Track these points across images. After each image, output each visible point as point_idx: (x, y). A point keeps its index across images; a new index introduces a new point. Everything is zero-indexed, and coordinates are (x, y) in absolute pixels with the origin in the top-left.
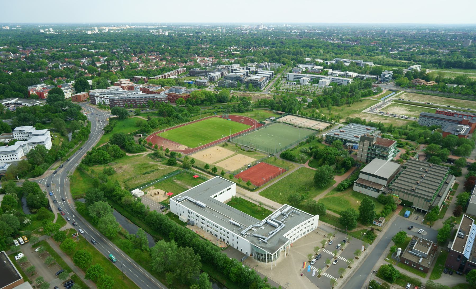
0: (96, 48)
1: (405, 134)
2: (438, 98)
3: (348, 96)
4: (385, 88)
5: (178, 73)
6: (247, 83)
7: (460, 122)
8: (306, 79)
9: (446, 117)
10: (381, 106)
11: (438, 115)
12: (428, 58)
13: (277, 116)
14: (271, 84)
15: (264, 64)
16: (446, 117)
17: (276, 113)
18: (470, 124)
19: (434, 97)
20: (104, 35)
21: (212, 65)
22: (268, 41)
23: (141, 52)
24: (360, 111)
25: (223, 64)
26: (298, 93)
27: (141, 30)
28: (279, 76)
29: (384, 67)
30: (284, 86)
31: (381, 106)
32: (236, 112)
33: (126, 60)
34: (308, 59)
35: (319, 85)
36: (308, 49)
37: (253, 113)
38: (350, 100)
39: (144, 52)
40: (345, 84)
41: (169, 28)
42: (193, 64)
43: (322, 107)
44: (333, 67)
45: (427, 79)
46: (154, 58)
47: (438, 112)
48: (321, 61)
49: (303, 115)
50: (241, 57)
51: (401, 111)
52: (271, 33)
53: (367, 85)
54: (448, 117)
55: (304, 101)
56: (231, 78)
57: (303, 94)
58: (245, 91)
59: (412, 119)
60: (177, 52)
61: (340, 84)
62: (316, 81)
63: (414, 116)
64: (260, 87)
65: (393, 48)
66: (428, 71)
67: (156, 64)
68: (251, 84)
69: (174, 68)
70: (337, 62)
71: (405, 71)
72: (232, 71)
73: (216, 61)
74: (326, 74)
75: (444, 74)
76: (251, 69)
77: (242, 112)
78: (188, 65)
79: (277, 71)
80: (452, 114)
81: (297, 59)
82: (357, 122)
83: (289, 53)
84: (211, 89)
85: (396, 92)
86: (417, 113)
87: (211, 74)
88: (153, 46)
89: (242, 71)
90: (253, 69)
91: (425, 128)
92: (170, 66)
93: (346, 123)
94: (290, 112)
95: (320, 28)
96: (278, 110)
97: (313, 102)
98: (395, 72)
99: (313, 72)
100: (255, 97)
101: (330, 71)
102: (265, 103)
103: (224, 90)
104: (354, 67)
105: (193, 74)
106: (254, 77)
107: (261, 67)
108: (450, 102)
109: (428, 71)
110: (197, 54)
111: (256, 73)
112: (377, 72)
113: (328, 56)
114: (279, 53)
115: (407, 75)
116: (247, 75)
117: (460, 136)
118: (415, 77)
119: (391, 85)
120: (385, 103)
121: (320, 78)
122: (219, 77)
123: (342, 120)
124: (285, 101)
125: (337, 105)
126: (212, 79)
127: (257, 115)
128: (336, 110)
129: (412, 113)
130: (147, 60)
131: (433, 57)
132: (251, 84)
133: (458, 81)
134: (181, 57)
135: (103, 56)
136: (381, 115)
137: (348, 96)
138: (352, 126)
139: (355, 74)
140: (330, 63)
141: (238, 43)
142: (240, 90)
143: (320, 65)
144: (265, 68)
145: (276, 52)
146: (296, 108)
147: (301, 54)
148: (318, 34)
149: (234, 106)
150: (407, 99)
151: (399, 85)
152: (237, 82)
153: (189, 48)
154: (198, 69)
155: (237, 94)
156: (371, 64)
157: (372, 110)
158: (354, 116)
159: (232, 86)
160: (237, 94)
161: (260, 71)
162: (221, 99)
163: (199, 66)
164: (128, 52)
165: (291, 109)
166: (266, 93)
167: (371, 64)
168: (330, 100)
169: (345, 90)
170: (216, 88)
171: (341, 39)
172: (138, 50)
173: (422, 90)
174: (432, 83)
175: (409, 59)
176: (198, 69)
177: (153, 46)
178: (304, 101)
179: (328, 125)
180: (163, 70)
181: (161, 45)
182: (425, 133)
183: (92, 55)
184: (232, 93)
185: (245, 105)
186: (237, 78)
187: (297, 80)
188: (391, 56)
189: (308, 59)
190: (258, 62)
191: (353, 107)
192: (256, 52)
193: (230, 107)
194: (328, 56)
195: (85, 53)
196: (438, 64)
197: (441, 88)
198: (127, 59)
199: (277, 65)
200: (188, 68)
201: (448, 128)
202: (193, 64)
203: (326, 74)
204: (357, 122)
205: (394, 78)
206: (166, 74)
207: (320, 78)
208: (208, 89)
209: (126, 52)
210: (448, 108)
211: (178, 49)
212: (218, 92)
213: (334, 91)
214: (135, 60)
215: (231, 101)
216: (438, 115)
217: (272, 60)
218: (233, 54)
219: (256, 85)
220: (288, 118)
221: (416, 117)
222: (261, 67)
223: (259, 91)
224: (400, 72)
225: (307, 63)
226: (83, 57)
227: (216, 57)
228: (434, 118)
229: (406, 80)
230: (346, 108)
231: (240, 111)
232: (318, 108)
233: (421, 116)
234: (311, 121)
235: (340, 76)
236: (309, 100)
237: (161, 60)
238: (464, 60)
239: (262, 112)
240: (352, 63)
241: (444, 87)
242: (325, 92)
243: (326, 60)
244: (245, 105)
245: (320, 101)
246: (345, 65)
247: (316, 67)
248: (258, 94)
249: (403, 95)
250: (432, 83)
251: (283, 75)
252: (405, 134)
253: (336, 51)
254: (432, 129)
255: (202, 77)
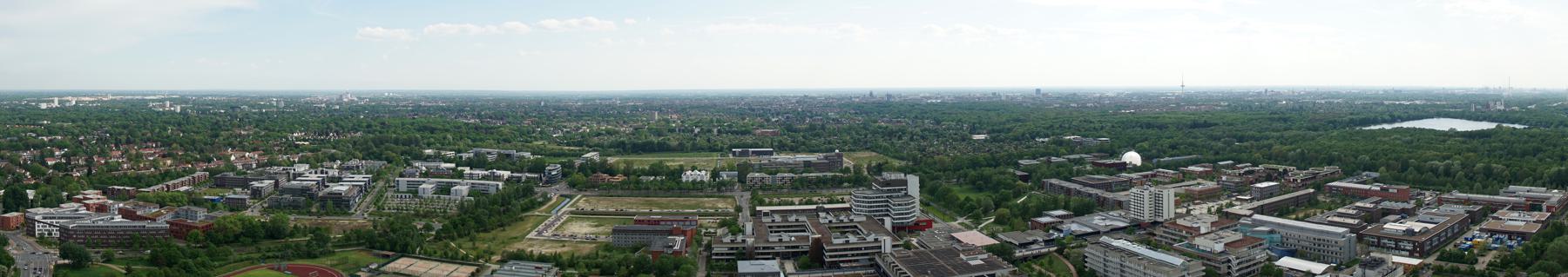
0: (50, 133)
1: (597, 266)
2: (633, 200)
3: (499, 213)
4: (554, 193)
5: (193, 182)
6: (324, 199)
7: (671, 233)
8: (428, 186)
9: (651, 228)
10: (553, 224)
11: (638, 227)
12: (607, 140)
13: (382, 261)
14: (368, 199)
15: (354, 163)
16: (651, 228)
17: (378, 255)
18: (684, 233)
19: (627, 199)
20: (68, 110)
21: (258, 166)
22: (360, 121)
23: (128, 142)
24: (523, 237)
25: (279, 165)
26: (417, 215)
27: (133, 103)
28: (381, 184)
29: (547, 160)
30: (392, 202)
31: (553, 224)
32: (301, 257)
33: (100, 155)
34: (428, 151)
35: (452, 197)
36: (427, 134)
37: (336, 257)
38: (504, 219)
39: (134, 143)
40: (493, 191)
41: (183, 100)
42: (222, 164)
43: (460, 236)
44: (471, 164)
45: (612, 172)
46: (151, 153)
47: (637, 222)
48: (451, 154)
49: (428, 256)
50: (312, 151)
51: (582, 229)
52: (364, 108)
53: (528, 191)
54: (654, 227)
55: (428, 228)
56: (293, 191)
57: (425, 216)
58: (318, 214)
59: (602, 238)
60: (194, 142)
61: (485, 193)
62: (445, 190)
63: (603, 232)
64: (348, 207)
65: (556, 128)
66: (611, 160)
67: (154, 164)
68: (330, 202)
69: (186, 172)
70: (476, 154)
71: (578, 162)
72: (296, 176)
73: (265, 159)
74: (461, 175)
75: (632, 163)
76: (331, 173)
77: (315, 257)
78: (212, 166)
79: (377, 176)
80: (657, 222)
81: (411, 152)
82: (519, 257)
83: (396, 142)
84: (253, 213)
85: (571, 197)
86: (609, 229)
87: (256, 184)
88: (152, 132)
89: (314, 177)
90: (334, 173)
91: (624, 251)
92: (180, 169)
93: (502, 262)
94: (405, 251)
95: (444, 99)
96: (383, 249)
97: (445, 229)
98: (563, 164)
99: (439, 174)
100: (339, 224)
101: (467, 170)
102: (358, 238)
103: (280, 215)
104: (504, 161)
105: (222, 183)
106: (336, 188)
107: (348, 168)
108: (651, 204)
109: (611, 160)
110: (230, 145)
111: (338, 180)
112: (538, 168)
113: (462, 145)
114: (379, 142)
115: (582, 168)
116: (322, 184)
117: (676, 253)
118: (594, 171)
119: (562, 187)
120: (558, 219)
121: (452, 185)
122: (271, 189)
123: (496, 258)
124: (394, 231)
125: (486, 231)
126: (256, 194)
127: (344, 262)
128: (483, 240)
129: (601, 229)
130: (139, 157)
131: (613, 138)
132: (330, 202)
133: (654, 171)
134: (201, 151)
135: (61, 148)
136: (557, 239)
137: (499, 213)
138: (512, 266)
139: (506, 174)
140: (465, 156)
141: (305, 126)
142: (310, 214)
143: (449, 161)
144: (356, 170)
145: (373, 141)
146: (414, 243)
147: (417, 142)
148: (443, 109)
149: (297, 245)
150: (588, 208)
151: (572, 185)
152: (306, 199)
153: (217, 136)
154: (231, 175)
155: (305, 221)
156: (527, 155)
157: (540, 233)
158: (515, 247)
159: (295, 207)
160: (305, 221)
161: (347, 175)
162: (274, 232)
163: (234, 169)
164: (105, 141)
165: (406, 245)
166: (360, 218)
167: (527, 155)
168: (472, 223)
169: (494, 202)
170: (265, 211)
171: (479, 116)
172: (123, 138)
173: (608, 190)
174: (620, 178)
175: (580, 144)
176: (231, 175)
177: (152, 132)
178: (428, 228)
179: (473, 269)
180: (167, 175)
181: (165, 129)
182: (626, 259)
183: (44, 145)
184: (292, 220)
185: (319, 243)
186: (304, 191)
187: (414, 191)
188: (554, 141)
189: (428, 151)
190: (342, 159)
191: (511, 232)
192: (338, 142)
193: (288, 247)
194: (462, 145)
195: (31, 141)
196: (622, 148)
197: (633, 184)
198: (102, 154)
199: (378, 163)
200: (213, 173)
201: (658, 244)
202: (222, 164)
203: (461, 175)
204: (519, 257)
205: (564, 175)
206: (170, 183)
207: (452, 185)
208: (248, 213)
209: (101, 141)
210: (651, 213)
211: (197, 137)
212: (267, 219)
213: (477, 204)
214: (115, 156)
215: (292, 235)
216: (638, 227)
217: (368, 155)
218: (297, 146)
219: (340, 204)
220: (401, 264)
221: (607, 234)
222: (348, 168)
223: (346, 214)
224: (571, 166)
225: (427, 158)
226: (27, 148)
227: (266, 152)
228: (634, 232)
229: (579, 177)
230: (501, 235)
231: (311, 256)
232: (453, 239)
233: (615, 231)
234: (443, 266)
235: (484, 178)
236: (437, 226)
237: (164, 156)
238: (655, 139)
239: (354, 255)
240: (499, 154)
241: (638, 182)
242: (461, 206)
243: (459, 151)
244: (319, 243)
245: (455, 226)
246: (490, 158)
247: (444, 165)
248: (344, 221)
249: (582, 202)
250: (620, 178)
251: (388, 181)
252: (597, 266)
253: (473, 135)
254: (635, 249)
255: (238, 190)
